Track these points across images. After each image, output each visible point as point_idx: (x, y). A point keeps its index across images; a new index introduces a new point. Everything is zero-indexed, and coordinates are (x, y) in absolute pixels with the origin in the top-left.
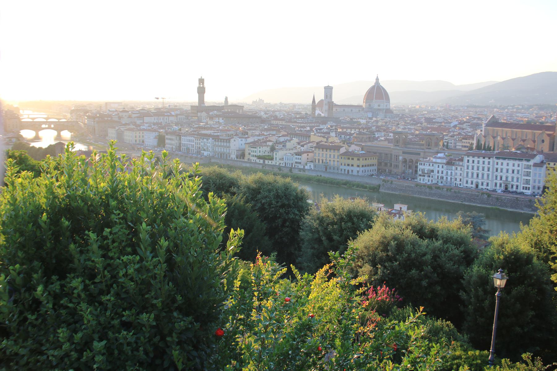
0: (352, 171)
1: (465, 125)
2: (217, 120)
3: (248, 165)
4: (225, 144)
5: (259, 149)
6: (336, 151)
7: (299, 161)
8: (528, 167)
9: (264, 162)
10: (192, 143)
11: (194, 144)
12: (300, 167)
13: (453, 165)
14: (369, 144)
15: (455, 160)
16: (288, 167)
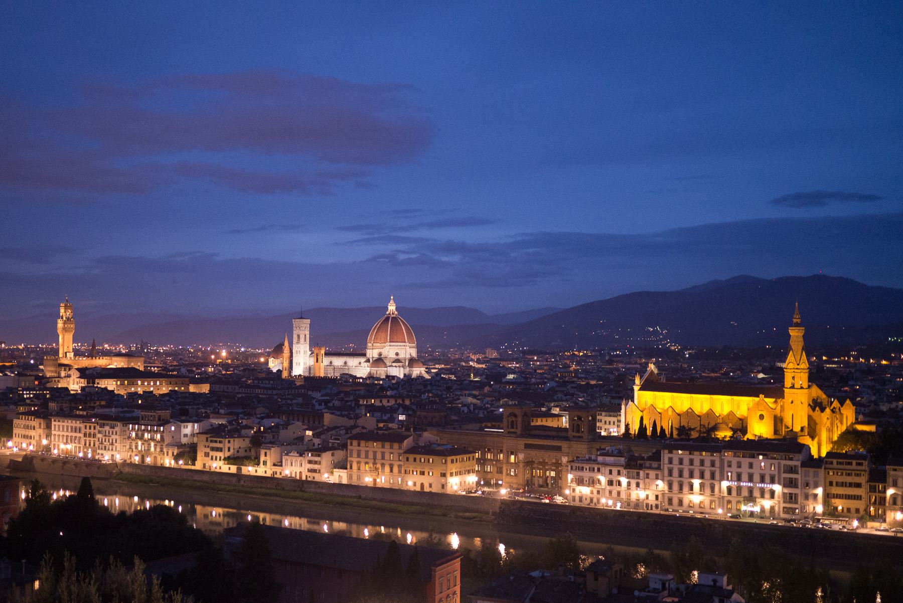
0: (430, 486)
1: (569, 387)
3: (206, 478)
5: (227, 445)
6: (396, 445)
8: (792, 470)
9: (239, 469)
11: (82, 435)
12: (317, 479)
13: (641, 467)
15: (643, 459)
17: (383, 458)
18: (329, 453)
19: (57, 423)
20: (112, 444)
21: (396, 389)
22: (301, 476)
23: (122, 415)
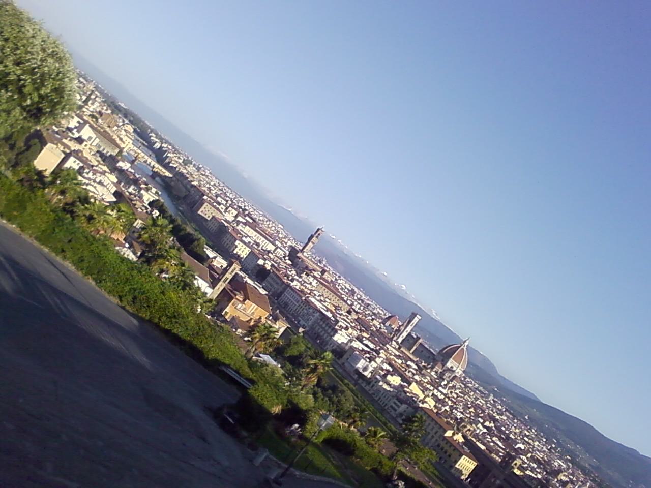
2: (311, 279)
4: (324, 326)
7: (396, 407)
10: (296, 303)
11: (297, 305)
12: (391, 413)
14: (474, 440)
16: (381, 406)
17: (432, 429)
18: (406, 406)
19: (290, 290)
20: (308, 320)
21: (445, 389)
22: (385, 406)
23: (322, 310)
